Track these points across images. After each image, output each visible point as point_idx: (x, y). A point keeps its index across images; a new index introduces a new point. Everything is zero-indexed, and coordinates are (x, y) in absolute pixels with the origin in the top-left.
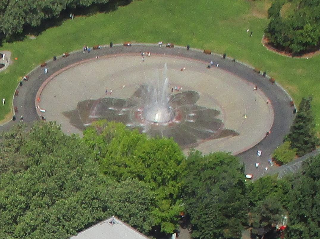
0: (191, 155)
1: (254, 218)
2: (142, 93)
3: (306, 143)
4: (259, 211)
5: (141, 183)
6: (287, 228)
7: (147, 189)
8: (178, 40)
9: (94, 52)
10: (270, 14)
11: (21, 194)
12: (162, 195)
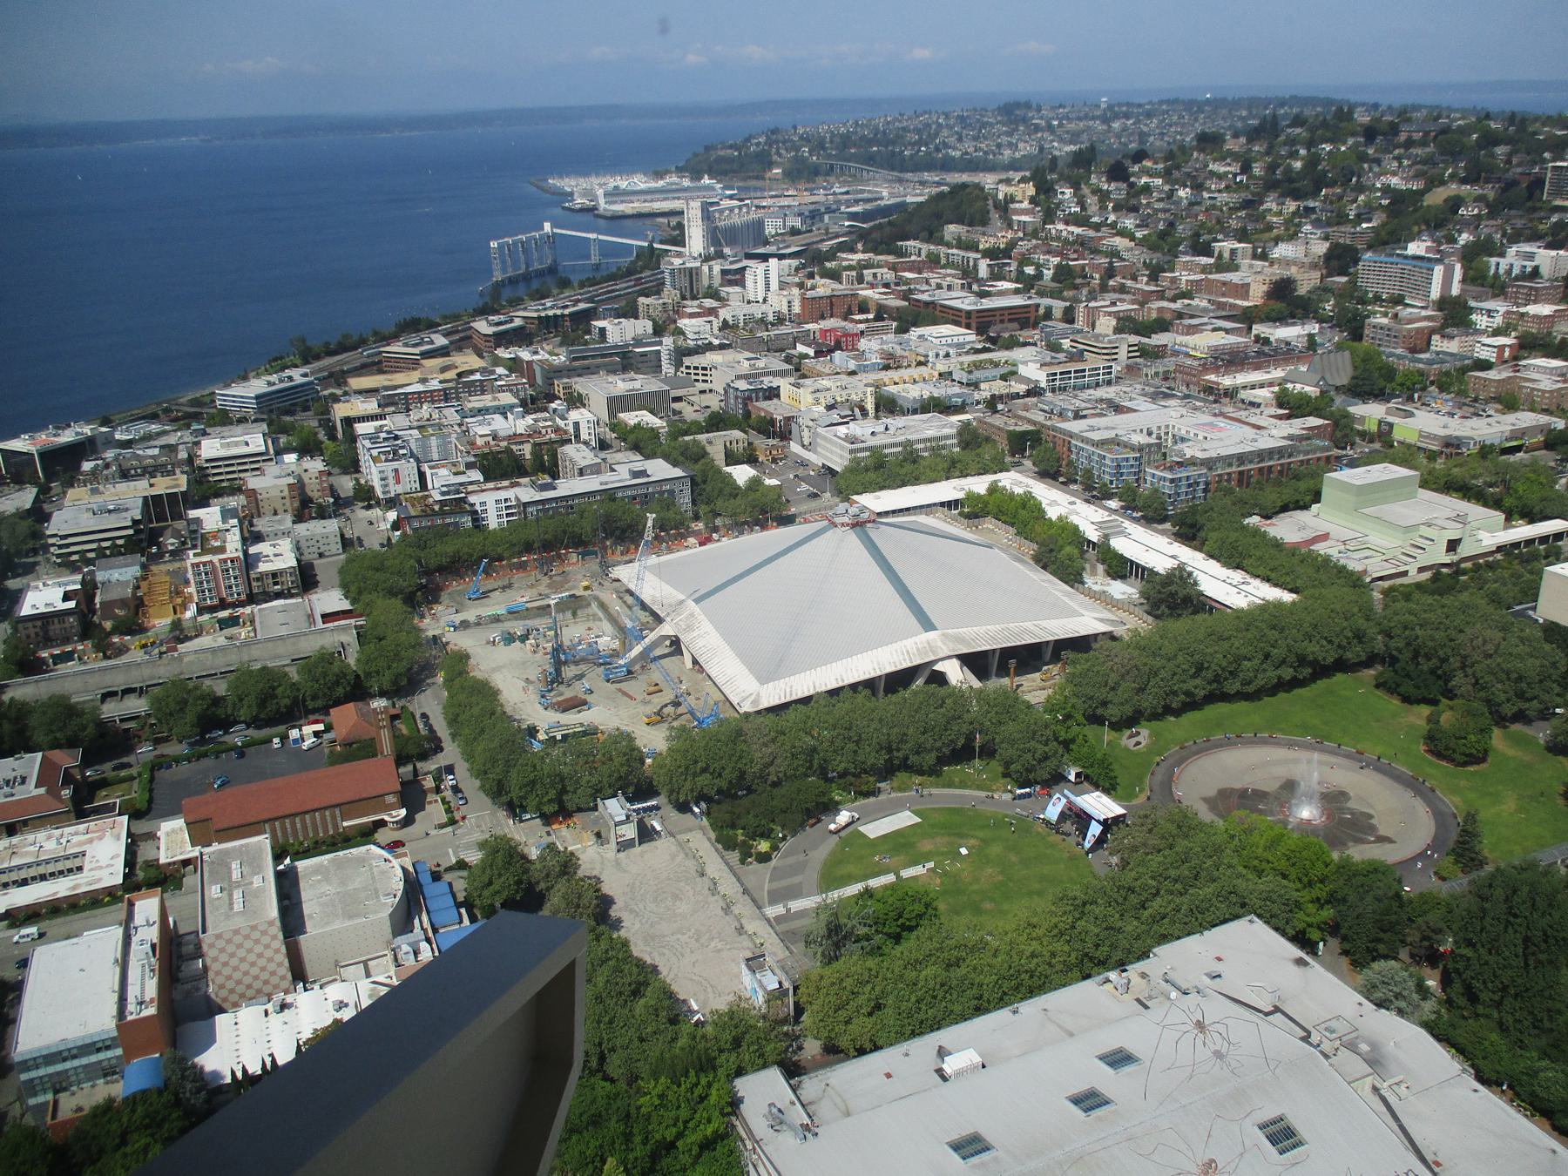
1: (1413, 936)
2: (1290, 786)
3: (1472, 860)
4: (1419, 928)
5: (1285, 882)
7: (1291, 890)
8: (1328, 738)
9: (1237, 740)
10: (1429, 720)
11: (1152, 878)
12: (1308, 898)
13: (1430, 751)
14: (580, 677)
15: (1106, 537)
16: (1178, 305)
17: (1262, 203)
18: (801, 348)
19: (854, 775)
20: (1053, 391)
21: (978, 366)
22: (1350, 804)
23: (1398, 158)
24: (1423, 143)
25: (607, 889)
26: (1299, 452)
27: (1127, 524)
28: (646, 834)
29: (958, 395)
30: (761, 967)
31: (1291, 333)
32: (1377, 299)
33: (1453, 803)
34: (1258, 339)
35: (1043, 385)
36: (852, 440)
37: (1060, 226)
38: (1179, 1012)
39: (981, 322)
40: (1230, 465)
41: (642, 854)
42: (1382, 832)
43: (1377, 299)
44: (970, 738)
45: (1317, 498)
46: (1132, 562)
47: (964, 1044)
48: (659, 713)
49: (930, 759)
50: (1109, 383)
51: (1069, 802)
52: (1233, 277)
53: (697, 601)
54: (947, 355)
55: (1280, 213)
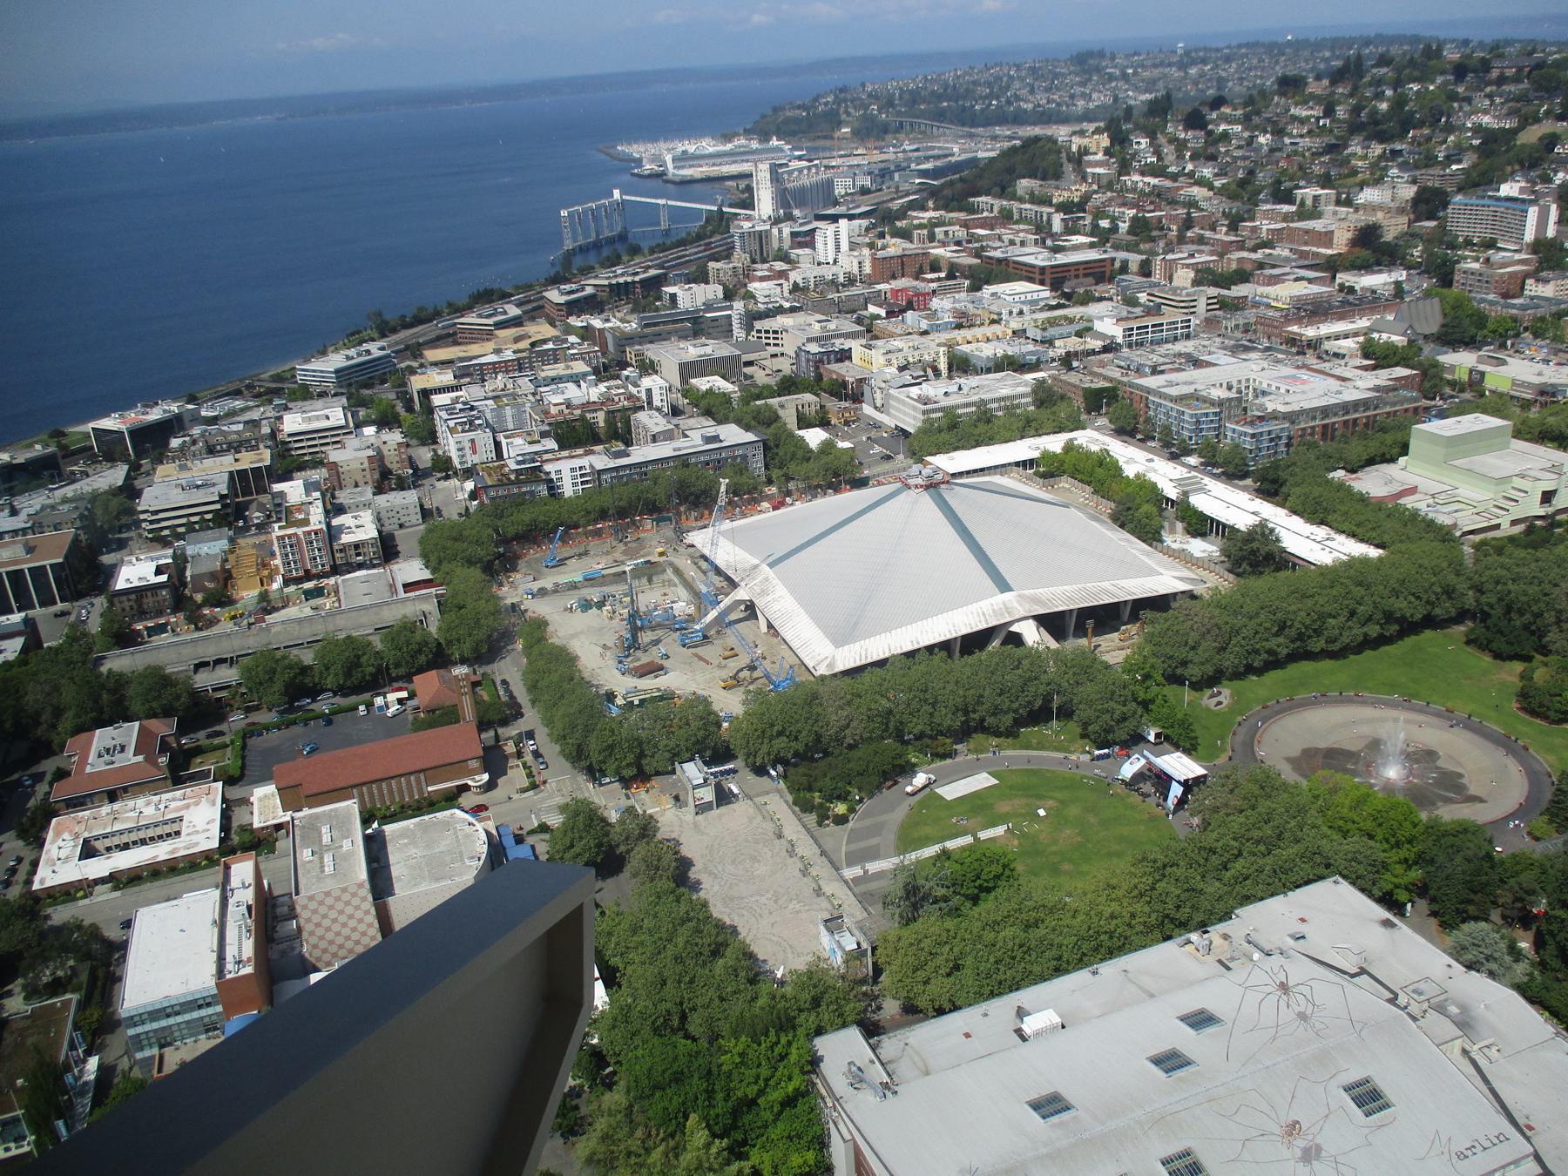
0: (1430, 819)
1: (1505, 897)
2: (1375, 745)
4: (1511, 890)
5: (1371, 843)
6: (1546, 913)
7: (1377, 850)
8: (1416, 696)
9: (1322, 699)
10: (1522, 677)
11: (1235, 839)
13: (1522, 709)
14: (656, 642)
15: (1186, 494)
16: (1259, 255)
17: (1346, 146)
18: (872, 309)
19: (931, 737)
20: (1130, 346)
21: (1052, 322)
22: (1439, 763)
23: (1490, 96)
24: (1517, 79)
25: (686, 851)
26: (1386, 404)
27: (1208, 481)
28: (723, 797)
29: (1032, 353)
30: (840, 927)
31: (1378, 281)
32: (1468, 243)
33: (1547, 762)
34: (1342, 288)
35: (1120, 340)
36: (925, 401)
37: (1136, 178)
38: (1263, 973)
39: (1056, 278)
40: (1314, 418)
41: (720, 817)
42: (1473, 790)
43: (1468, 243)
44: (1047, 699)
45: (1404, 450)
46: (1212, 520)
47: (1044, 1005)
48: (734, 677)
49: (1007, 720)
50: (1188, 337)
51: (1149, 762)
52: (1317, 225)
53: (771, 565)
54: (1021, 313)
55: (1365, 157)
